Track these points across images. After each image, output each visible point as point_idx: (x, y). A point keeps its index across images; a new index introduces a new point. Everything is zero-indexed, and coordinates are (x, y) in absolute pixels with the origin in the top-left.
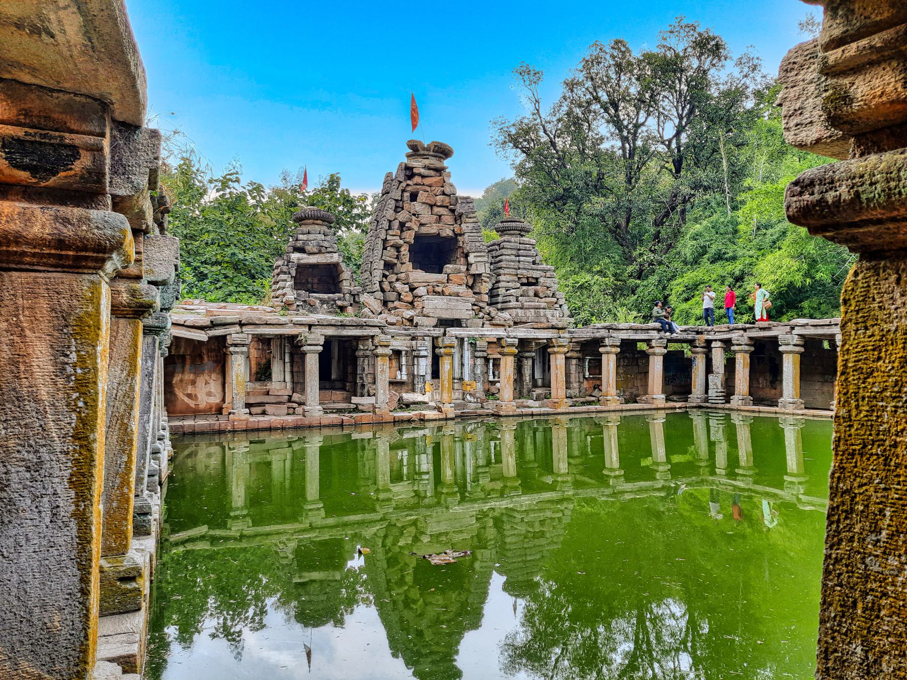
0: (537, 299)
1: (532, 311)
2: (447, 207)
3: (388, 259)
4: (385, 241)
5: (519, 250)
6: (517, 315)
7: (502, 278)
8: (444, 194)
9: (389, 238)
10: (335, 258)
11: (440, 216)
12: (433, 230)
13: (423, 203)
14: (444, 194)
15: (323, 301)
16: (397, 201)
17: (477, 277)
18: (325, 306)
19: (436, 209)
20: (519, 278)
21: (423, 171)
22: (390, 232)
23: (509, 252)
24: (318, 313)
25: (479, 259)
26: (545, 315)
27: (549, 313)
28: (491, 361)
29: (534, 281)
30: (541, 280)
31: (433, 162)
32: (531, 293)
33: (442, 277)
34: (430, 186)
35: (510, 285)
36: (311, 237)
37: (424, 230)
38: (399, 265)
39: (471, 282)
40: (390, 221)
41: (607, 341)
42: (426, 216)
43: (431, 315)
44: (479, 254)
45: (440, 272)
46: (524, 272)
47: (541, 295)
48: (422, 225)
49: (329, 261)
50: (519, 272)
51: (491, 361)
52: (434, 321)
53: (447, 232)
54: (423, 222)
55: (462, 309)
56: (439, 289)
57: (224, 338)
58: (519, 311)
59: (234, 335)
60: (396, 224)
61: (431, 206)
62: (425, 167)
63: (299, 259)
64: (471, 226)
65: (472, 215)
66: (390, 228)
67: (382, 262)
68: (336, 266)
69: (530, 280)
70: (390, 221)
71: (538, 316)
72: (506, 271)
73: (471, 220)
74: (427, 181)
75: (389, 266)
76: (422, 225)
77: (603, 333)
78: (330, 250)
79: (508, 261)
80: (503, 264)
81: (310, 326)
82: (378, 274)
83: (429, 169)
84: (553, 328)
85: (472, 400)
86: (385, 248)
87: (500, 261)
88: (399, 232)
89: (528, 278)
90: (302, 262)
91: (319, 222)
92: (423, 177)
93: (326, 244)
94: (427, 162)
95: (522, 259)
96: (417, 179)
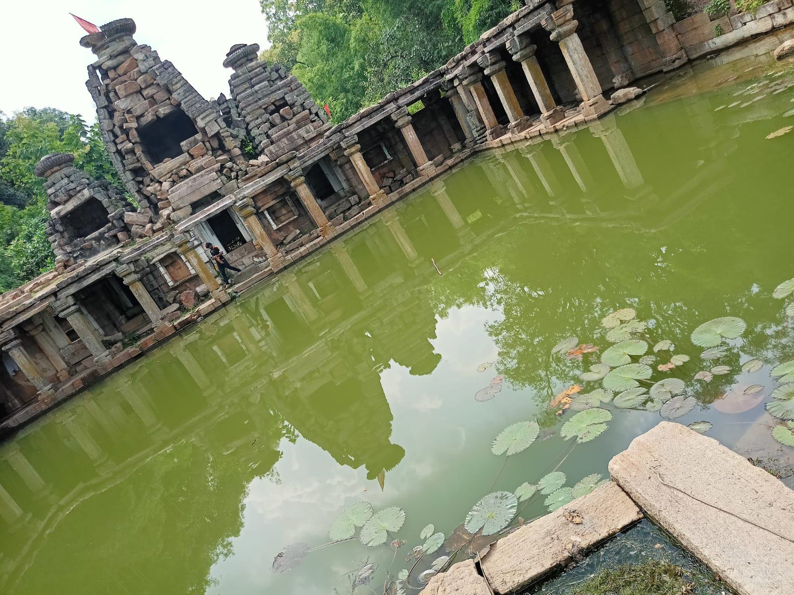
0: (285, 123)
1: (285, 140)
2: (152, 84)
3: (131, 167)
4: (118, 152)
5: (251, 79)
6: (271, 153)
7: (248, 119)
8: (141, 73)
9: (119, 147)
10: (87, 193)
11: (152, 97)
12: (149, 117)
13: (126, 97)
14: (141, 73)
15: (97, 239)
16: (105, 107)
17: (217, 135)
18: (102, 242)
19: (145, 93)
20: (264, 109)
21: (110, 63)
22: (118, 141)
23: (242, 88)
24: (99, 252)
25: (208, 119)
26: (299, 136)
27: (302, 131)
28: (266, 212)
29: (282, 102)
30: (288, 98)
31: (118, 46)
33: (183, 157)
34: (125, 74)
35: (259, 121)
36: (57, 186)
38: (143, 166)
39: (215, 144)
40: (112, 131)
41: (343, 145)
42: (139, 105)
43: (182, 206)
44: (204, 115)
45: (181, 152)
46: (266, 100)
47: (287, 117)
49: (83, 199)
50: (260, 103)
51: (266, 212)
53: (164, 110)
54: (138, 113)
55: (209, 182)
56: (184, 172)
58: (271, 147)
60: (117, 131)
61: (140, 92)
62: (111, 57)
63: (58, 213)
64: (181, 91)
65: (175, 80)
67: (128, 173)
68: (92, 201)
69: (277, 104)
70: (112, 131)
71: (292, 140)
72: (249, 109)
73: (179, 85)
74: (121, 70)
75: (138, 172)
76: (138, 118)
77: (336, 138)
78: (78, 189)
79: (246, 97)
80: (241, 105)
81: (54, 294)
82: (131, 186)
83: (116, 56)
85: (261, 259)
86: (123, 158)
87: (239, 102)
88: (124, 136)
89: (273, 103)
90: (62, 214)
91: (55, 169)
92: (115, 68)
93: (72, 186)
95: (257, 87)
96: (111, 74)
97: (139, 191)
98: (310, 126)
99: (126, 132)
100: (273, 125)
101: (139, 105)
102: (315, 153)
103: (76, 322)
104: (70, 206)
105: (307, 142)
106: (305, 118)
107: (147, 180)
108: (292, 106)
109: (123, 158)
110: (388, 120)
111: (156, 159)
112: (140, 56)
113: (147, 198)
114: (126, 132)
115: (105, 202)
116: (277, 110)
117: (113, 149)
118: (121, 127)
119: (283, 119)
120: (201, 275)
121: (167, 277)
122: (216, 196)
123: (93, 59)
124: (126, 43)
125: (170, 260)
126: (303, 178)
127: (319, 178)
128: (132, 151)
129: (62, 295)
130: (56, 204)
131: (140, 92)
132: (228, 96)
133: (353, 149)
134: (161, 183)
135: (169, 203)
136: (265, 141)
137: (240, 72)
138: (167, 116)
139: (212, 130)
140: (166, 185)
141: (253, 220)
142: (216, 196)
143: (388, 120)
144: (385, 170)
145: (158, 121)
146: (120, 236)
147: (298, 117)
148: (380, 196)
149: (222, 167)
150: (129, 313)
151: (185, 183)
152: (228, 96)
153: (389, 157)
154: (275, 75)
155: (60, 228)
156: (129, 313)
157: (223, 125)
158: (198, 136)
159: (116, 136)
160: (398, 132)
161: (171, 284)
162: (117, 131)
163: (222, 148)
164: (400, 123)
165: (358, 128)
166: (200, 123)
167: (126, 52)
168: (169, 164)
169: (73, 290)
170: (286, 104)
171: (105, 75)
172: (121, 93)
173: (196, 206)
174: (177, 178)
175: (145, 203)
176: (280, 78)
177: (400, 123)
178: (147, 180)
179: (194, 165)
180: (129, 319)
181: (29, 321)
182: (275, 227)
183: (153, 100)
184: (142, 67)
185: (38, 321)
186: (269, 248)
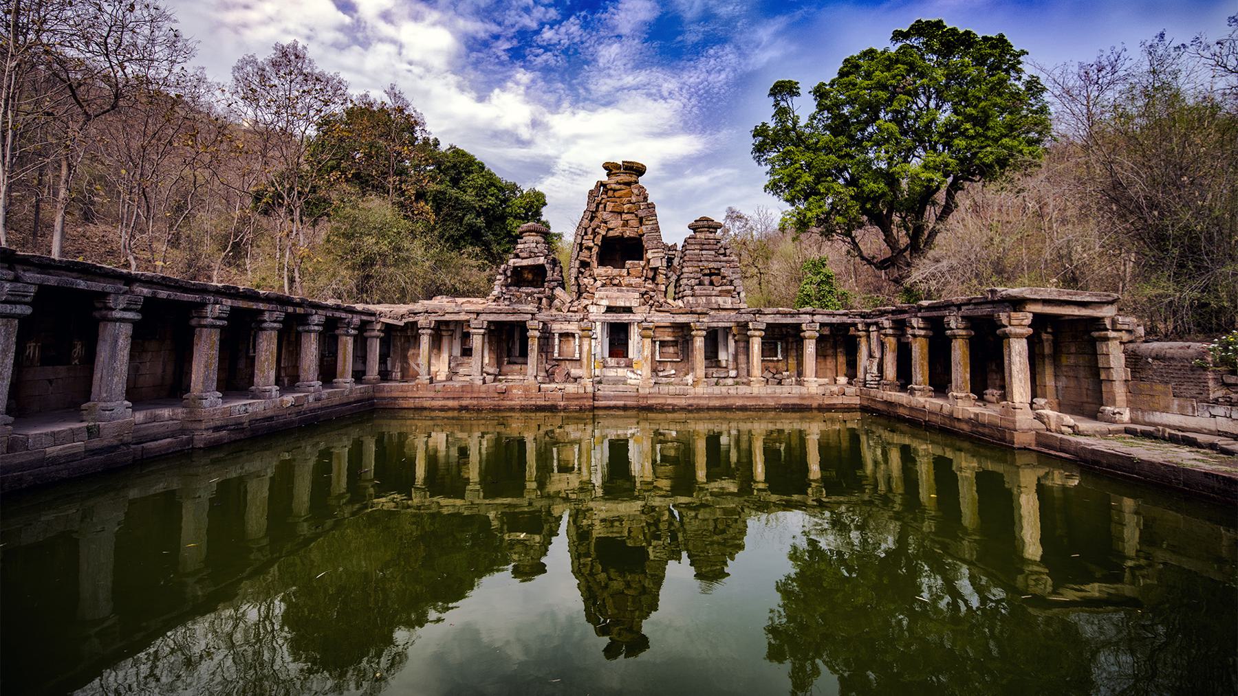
4: (581, 244)
7: (685, 270)
8: (630, 202)
10: (542, 260)
15: (528, 295)
17: (655, 270)
19: (624, 216)
27: (720, 300)
32: (706, 282)
33: (624, 272)
37: (611, 234)
39: (651, 274)
46: (706, 264)
48: (609, 229)
52: (603, 310)
55: (632, 299)
57: (416, 323)
59: (422, 320)
60: (590, 231)
66: (586, 234)
71: (709, 303)
74: (617, 194)
75: (585, 264)
76: (609, 229)
81: (478, 314)
82: (574, 271)
84: (692, 313)
86: (581, 250)
92: (615, 190)
94: (618, 179)
96: (610, 193)
97: (576, 278)
98: (729, 300)
99: (595, 233)
100: (701, 283)
101: (615, 223)
102: (723, 320)
103: (477, 342)
104: (525, 263)
105: (719, 309)
106: (729, 292)
107: (587, 273)
108: (724, 277)
109: (581, 250)
110: (798, 327)
111: (602, 263)
112: (636, 191)
113: (579, 285)
114: (595, 233)
115: (549, 273)
116: (710, 275)
117: (579, 241)
118: (594, 230)
119: (711, 283)
120: (585, 361)
121: (556, 348)
122: (628, 310)
123: (605, 179)
124: (633, 179)
125: (566, 336)
126: (704, 333)
127: (714, 339)
128: (590, 249)
129: (482, 317)
130: (517, 256)
131: (620, 213)
132: (679, 248)
133: (757, 333)
134: (595, 280)
135: (593, 298)
136: (688, 292)
137: (698, 235)
138: (630, 238)
139: (653, 264)
140: (599, 283)
141: (648, 341)
142: (628, 310)
143: (798, 327)
144: (771, 365)
145: (620, 239)
146: (544, 300)
147: (724, 288)
148: (759, 382)
149: (646, 293)
150: (512, 359)
151: (612, 292)
152: (679, 248)
153: (780, 357)
154: (722, 251)
155: (509, 273)
156: (512, 359)
157: (665, 264)
158: (642, 263)
159: (586, 234)
160: (802, 339)
161: (556, 355)
162: (590, 231)
163: (654, 279)
164: (807, 334)
165: (769, 319)
166: (649, 255)
167: (629, 184)
168: (610, 270)
169: (492, 318)
170: (718, 274)
171: (606, 192)
172: (609, 208)
173: (610, 309)
174: (610, 282)
175: (575, 288)
176: (725, 255)
177: (807, 334)
178: (587, 273)
179: (626, 281)
180: (509, 363)
181: (447, 323)
182: (658, 358)
183: (626, 223)
184: (634, 199)
185: (452, 327)
186: (646, 371)
